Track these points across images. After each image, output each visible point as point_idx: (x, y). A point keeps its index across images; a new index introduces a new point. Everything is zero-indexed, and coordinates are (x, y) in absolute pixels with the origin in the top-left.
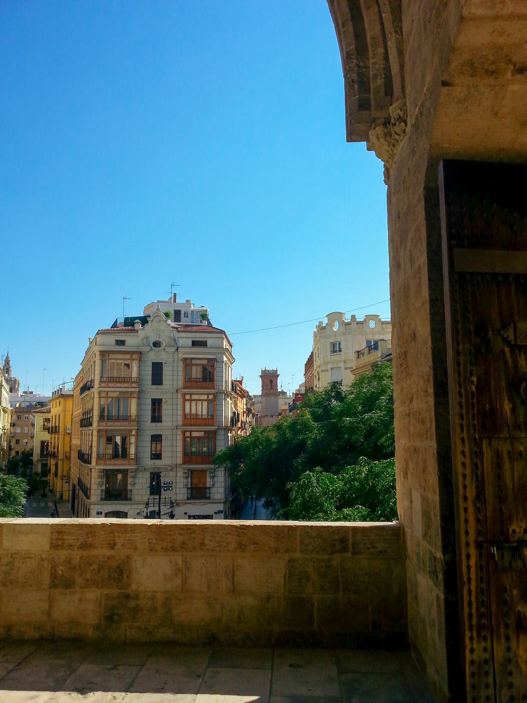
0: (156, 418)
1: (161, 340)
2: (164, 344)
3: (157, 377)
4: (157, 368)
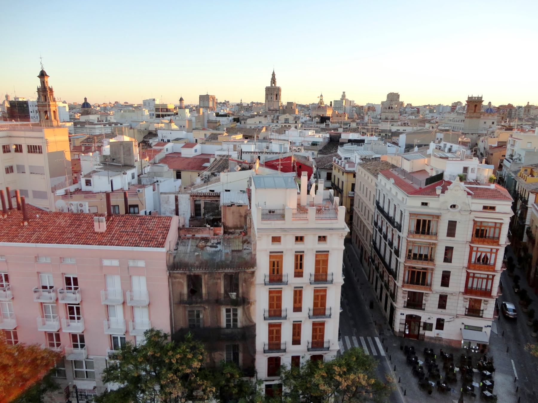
0: (448, 259)
2: (459, 208)
3: (451, 232)
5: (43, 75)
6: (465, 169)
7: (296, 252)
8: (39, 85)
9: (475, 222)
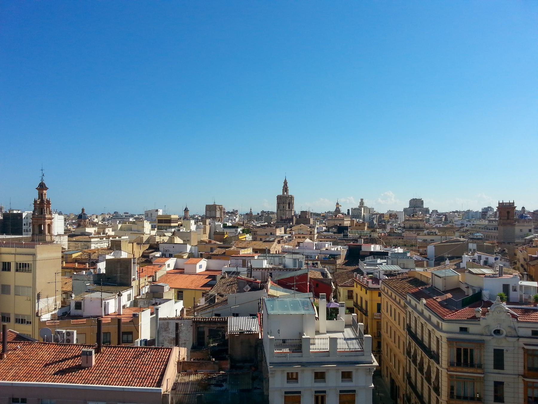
1: (501, 329)
2: (505, 333)
3: (499, 363)
4: (499, 355)
5: (42, 187)
6: (506, 288)
7: (316, 392)
8: (37, 197)
9: (526, 351)
